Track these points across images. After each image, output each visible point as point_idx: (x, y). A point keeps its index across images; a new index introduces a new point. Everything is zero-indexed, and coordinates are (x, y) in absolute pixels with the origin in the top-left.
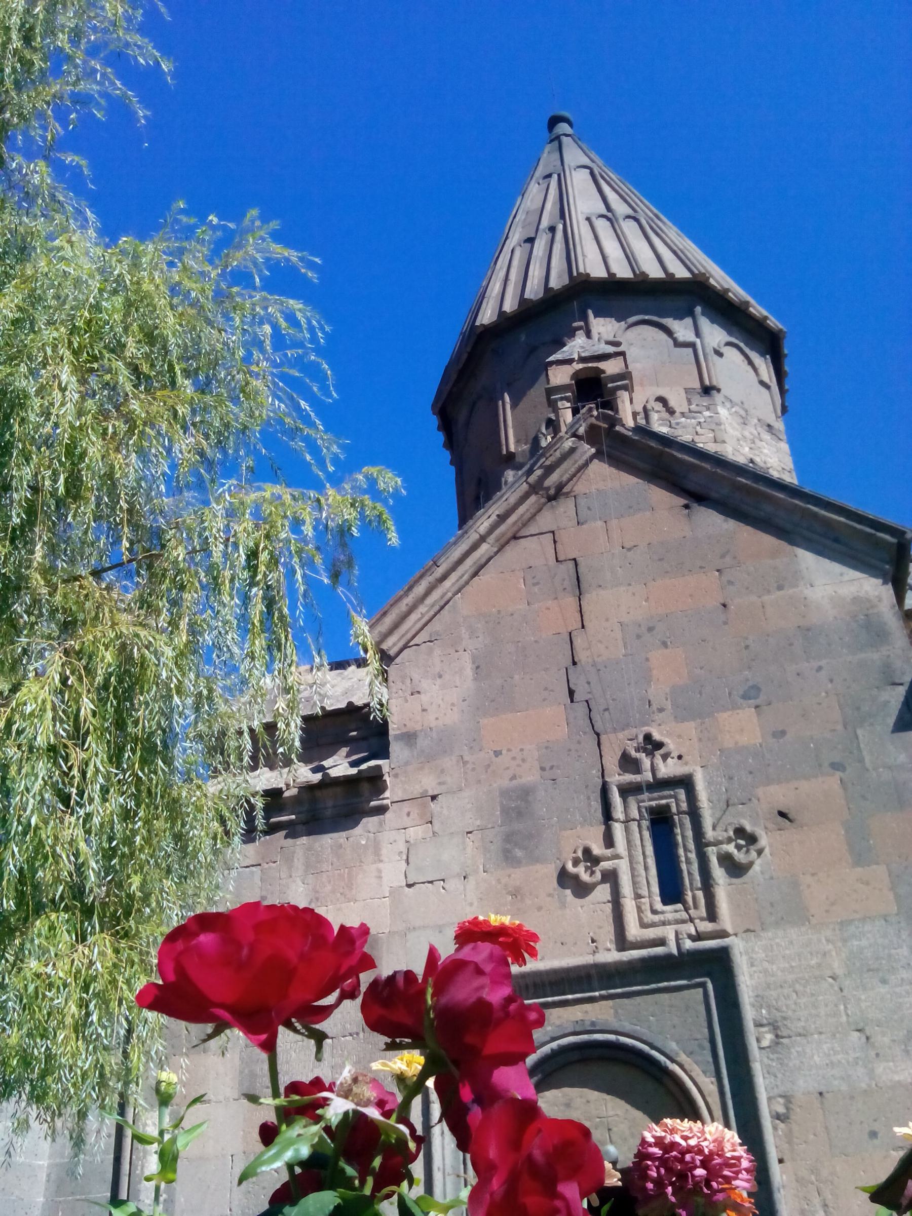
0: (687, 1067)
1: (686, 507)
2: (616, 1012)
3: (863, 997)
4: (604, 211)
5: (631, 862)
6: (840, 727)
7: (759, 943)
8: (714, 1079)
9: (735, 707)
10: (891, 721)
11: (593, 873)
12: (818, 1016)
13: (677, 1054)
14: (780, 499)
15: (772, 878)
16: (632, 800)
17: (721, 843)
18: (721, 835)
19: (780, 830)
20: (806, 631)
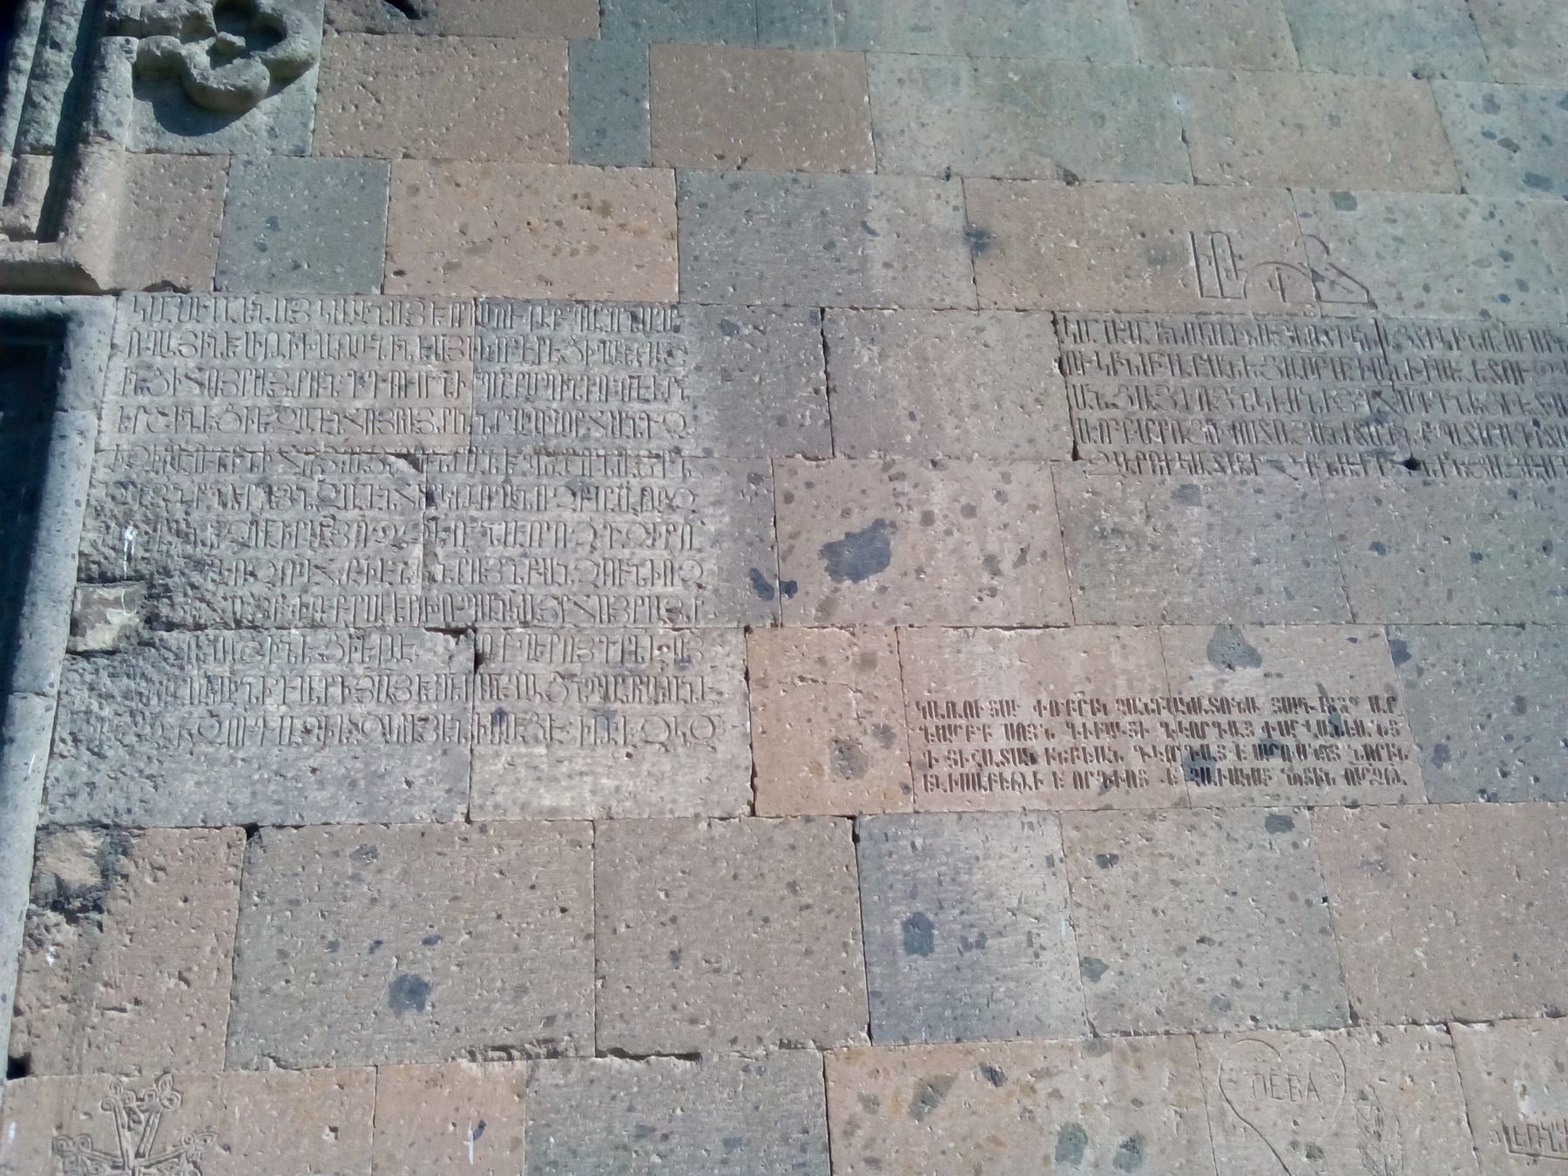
19: (370, 31)
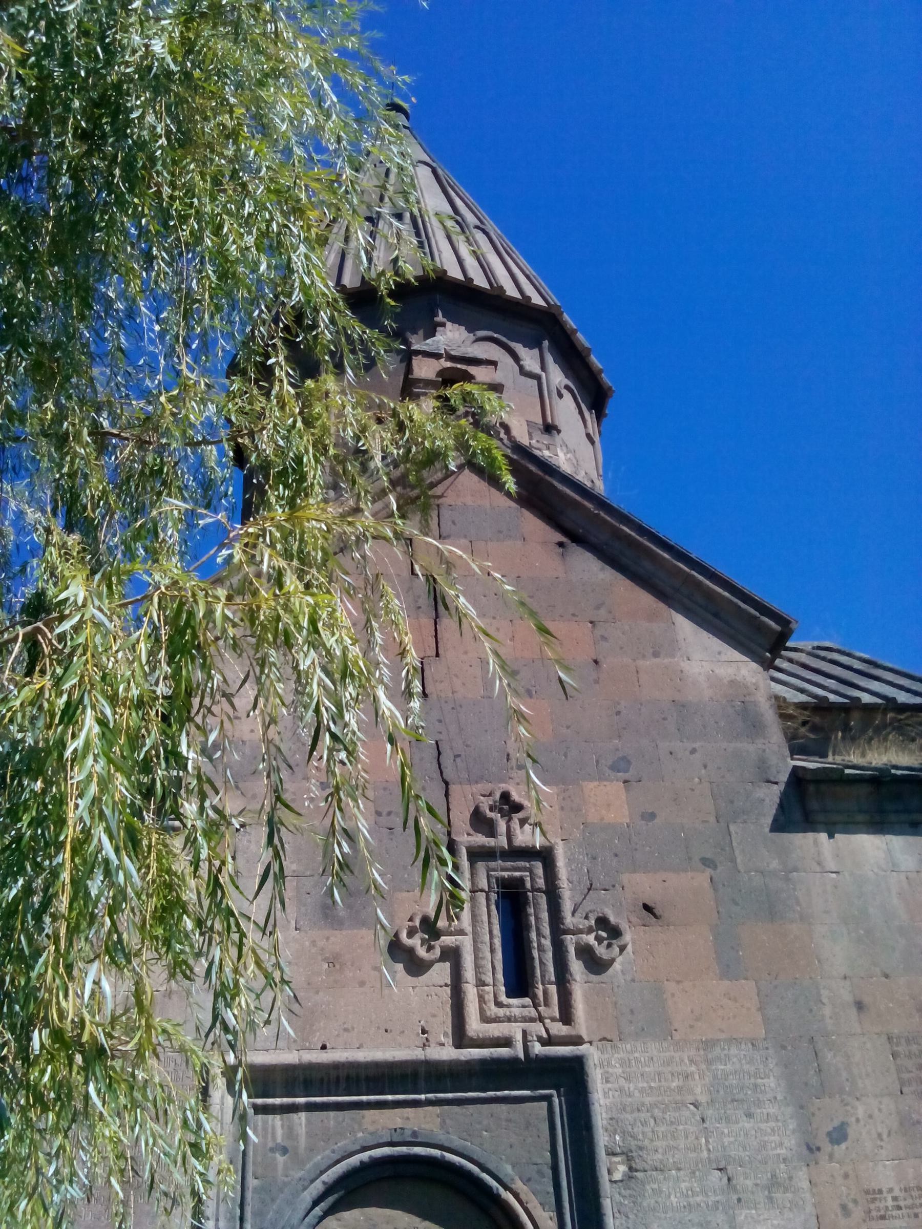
0: (523, 1197)
1: (561, 545)
2: (443, 1124)
3: (726, 1131)
4: (452, 213)
5: (475, 941)
6: (712, 819)
7: (616, 1055)
8: (553, 1214)
9: (601, 778)
10: (769, 820)
11: (429, 950)
12: (677, 1148)
13: (513, 1180)
14: (664, 558)
15: (633, 980)
16: (481, 866)
17: (580, 932)
18: (583, 924)
19: (644, 926)
20: (681, 706)
